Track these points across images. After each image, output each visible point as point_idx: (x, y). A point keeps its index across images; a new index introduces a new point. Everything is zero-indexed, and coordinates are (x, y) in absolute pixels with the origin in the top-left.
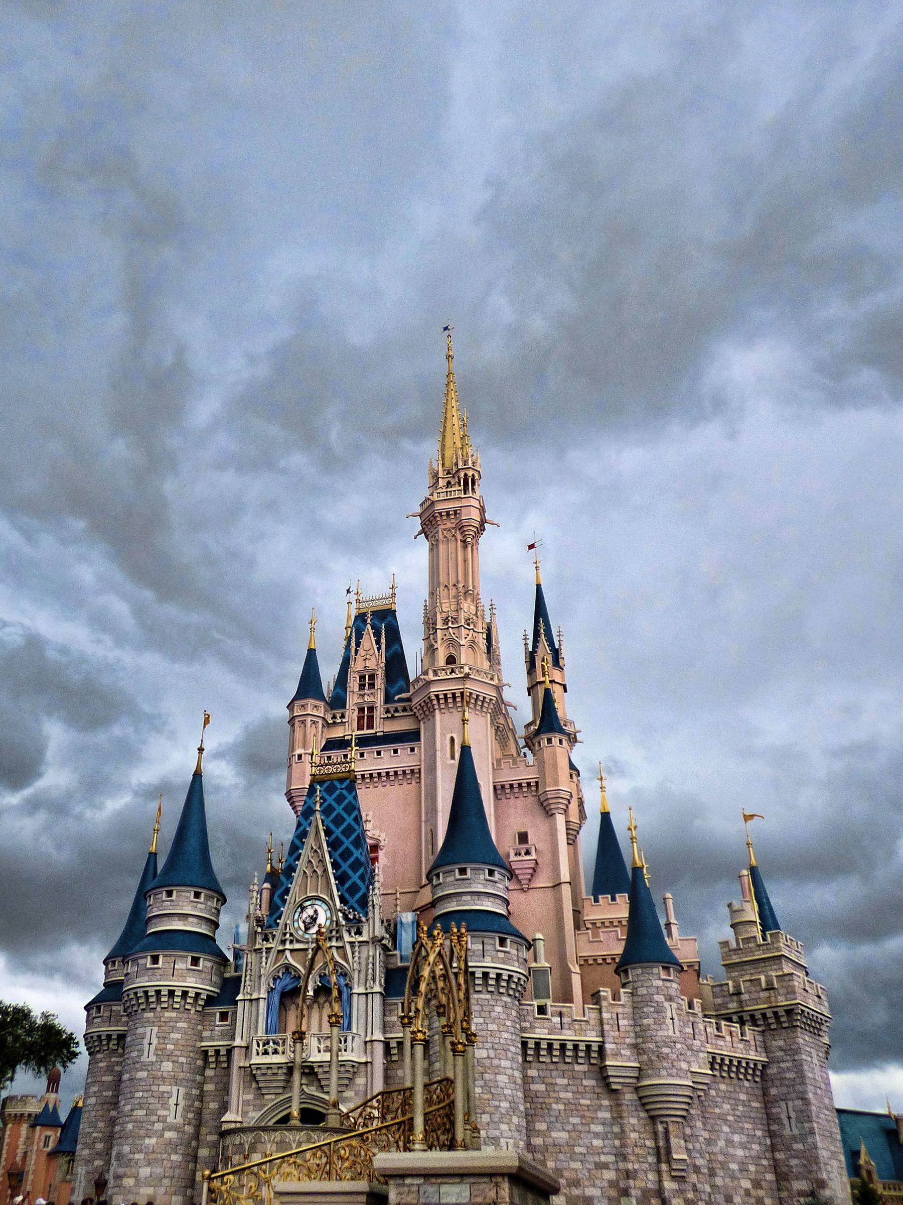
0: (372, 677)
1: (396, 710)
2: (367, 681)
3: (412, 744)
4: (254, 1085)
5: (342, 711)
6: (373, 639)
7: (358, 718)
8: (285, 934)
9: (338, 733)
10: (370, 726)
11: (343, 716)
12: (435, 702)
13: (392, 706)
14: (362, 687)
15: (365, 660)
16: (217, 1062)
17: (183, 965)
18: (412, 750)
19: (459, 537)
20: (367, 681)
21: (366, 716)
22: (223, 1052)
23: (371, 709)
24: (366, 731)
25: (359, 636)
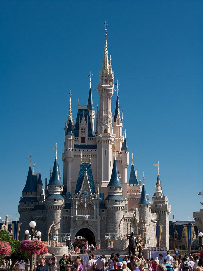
0: (84, 129)
1: (91, 139)
2: (83, 130)
3: (95, 149)
4: (76, 224)
5: (78, 137)
6: (85, 119)
7: (81, 140)
8: (80, 197)
9: (77, 143)
10: (84, 142)
11: (78, 139)
12: (102, 141)
13: (90, 138)
14: (82, 132)
15: (83, 125)
16: (66, 219)
17: (60, 201)
18: (95, 150)
19: (108, 97)
20: (83, 130)
21: (83, 140)
22: (67, 217)
23: (84, 138)
24: (83, 144)
25: (81, 118)
